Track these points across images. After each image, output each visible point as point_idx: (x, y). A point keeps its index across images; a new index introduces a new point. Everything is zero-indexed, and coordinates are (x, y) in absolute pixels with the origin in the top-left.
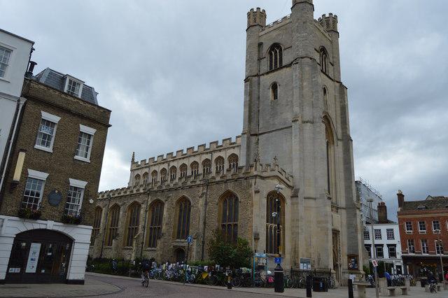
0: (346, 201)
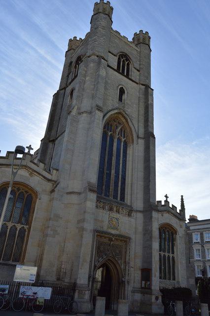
0: (144, 203)
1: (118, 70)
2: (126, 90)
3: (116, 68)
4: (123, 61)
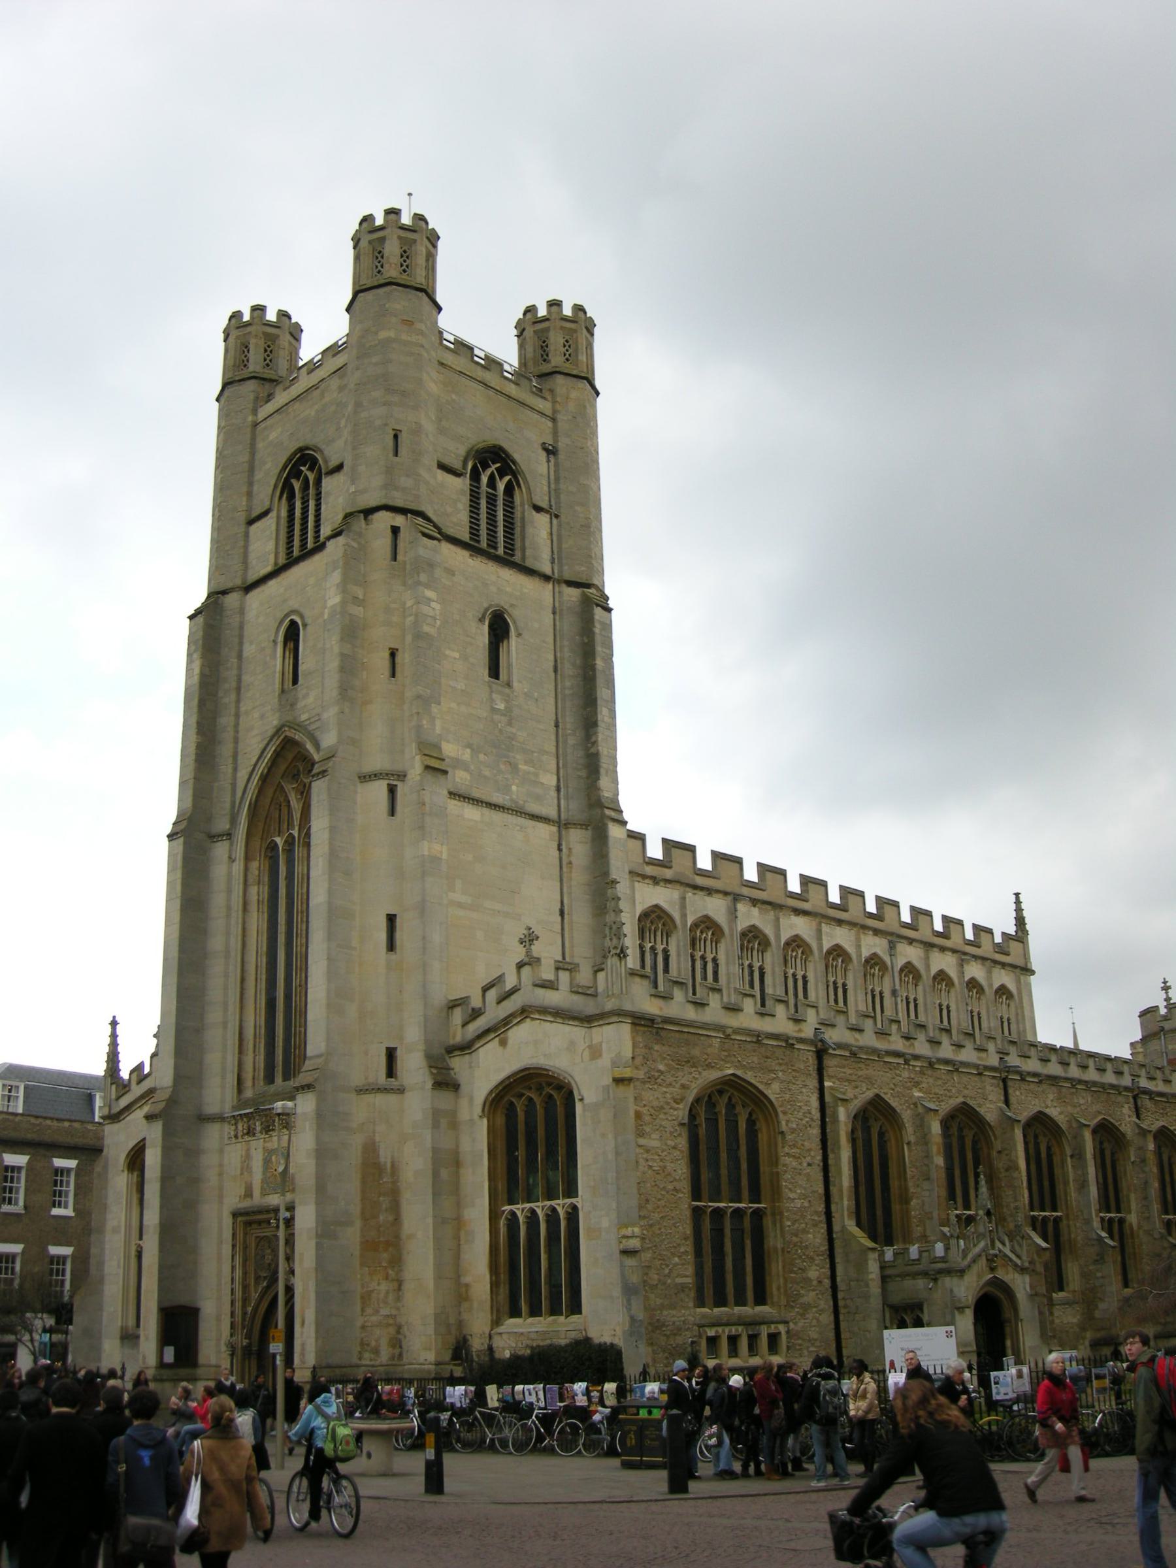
1: (472, 547)
2: (514, 622)
3: (465, 536)
4: (492, 483)
